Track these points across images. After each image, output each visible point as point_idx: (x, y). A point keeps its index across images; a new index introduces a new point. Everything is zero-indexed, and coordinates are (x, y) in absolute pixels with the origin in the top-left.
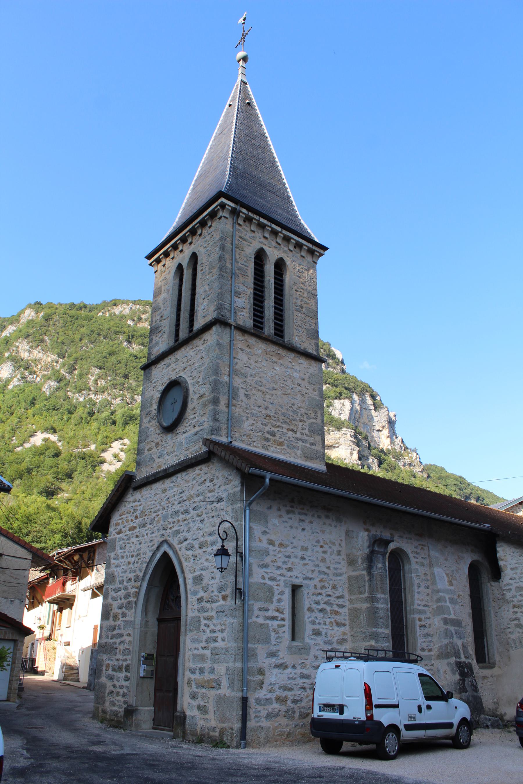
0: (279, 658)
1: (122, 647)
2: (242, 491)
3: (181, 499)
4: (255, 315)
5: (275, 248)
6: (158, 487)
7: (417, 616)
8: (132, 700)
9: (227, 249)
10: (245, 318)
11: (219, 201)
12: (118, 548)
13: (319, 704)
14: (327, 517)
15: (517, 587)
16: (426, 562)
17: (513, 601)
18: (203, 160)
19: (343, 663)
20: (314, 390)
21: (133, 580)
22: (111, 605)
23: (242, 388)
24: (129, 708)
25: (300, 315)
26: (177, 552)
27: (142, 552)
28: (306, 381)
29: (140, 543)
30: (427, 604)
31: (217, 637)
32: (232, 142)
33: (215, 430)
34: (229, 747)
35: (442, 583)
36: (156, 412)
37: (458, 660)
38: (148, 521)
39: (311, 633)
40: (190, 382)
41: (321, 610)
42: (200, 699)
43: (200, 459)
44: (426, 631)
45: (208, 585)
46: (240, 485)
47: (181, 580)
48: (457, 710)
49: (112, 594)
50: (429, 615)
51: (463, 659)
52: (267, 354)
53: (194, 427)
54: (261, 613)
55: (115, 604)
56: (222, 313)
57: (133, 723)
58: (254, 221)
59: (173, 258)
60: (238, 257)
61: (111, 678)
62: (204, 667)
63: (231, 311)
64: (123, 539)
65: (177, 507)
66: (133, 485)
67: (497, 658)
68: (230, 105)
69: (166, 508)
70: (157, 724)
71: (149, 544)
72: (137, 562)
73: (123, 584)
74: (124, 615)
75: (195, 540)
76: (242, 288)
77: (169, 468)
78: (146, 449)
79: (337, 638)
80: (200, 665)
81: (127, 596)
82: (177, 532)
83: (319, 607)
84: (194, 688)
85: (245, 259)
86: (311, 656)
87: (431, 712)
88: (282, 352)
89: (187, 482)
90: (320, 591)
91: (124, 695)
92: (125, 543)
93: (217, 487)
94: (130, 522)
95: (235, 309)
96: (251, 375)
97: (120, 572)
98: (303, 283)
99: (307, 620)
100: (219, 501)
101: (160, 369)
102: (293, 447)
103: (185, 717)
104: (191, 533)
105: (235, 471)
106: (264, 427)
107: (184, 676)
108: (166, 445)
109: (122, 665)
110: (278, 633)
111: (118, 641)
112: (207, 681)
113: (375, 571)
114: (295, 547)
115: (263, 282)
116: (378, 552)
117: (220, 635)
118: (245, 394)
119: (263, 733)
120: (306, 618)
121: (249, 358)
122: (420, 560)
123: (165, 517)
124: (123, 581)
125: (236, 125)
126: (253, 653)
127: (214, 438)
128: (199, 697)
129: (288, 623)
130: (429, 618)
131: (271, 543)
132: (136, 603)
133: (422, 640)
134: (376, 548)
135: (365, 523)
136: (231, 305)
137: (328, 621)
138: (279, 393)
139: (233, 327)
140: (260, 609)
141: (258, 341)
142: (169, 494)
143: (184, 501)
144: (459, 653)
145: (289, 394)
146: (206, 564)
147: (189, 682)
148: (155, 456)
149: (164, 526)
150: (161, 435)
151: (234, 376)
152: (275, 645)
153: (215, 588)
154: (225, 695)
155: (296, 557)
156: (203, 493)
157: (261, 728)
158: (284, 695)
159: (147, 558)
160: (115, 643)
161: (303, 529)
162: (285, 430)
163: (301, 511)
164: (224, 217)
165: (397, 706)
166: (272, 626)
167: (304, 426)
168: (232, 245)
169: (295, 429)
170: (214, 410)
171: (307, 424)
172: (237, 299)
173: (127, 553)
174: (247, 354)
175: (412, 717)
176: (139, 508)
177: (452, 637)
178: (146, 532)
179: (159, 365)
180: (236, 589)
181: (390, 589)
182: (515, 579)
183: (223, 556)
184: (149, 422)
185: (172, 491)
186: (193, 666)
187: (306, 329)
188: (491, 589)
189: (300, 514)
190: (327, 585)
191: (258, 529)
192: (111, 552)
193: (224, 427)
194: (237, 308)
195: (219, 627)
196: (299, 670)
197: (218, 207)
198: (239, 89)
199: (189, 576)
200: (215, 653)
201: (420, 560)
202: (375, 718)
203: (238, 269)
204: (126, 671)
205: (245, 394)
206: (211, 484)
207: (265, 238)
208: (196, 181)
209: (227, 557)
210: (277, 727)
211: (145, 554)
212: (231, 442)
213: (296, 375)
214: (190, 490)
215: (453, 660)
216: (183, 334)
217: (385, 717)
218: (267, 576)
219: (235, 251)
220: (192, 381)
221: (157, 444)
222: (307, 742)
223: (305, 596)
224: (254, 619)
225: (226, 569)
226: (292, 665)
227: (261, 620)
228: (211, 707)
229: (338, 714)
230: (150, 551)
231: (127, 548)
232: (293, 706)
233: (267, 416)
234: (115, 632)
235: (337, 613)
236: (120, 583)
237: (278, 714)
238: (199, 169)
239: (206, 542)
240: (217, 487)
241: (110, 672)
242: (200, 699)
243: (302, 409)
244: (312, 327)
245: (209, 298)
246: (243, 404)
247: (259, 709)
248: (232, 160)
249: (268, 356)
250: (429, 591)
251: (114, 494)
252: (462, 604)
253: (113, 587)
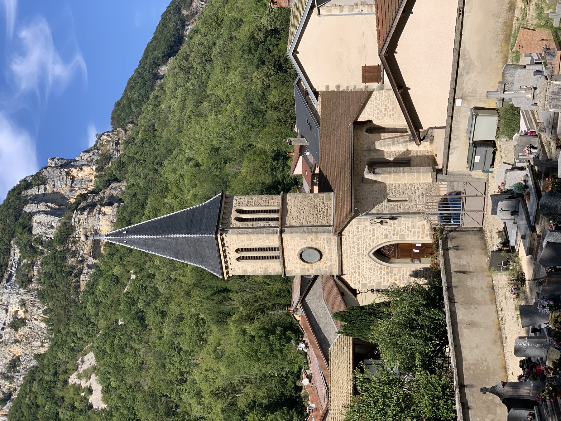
51: (408, 139)
81: (387, 274)
82: (366, 249)
84: (424, 236)
117: (407, 225)
123: (358, 255)
129: (401, 203)
147: (422, 238)
196: (417, 199)
200: (413, 227)
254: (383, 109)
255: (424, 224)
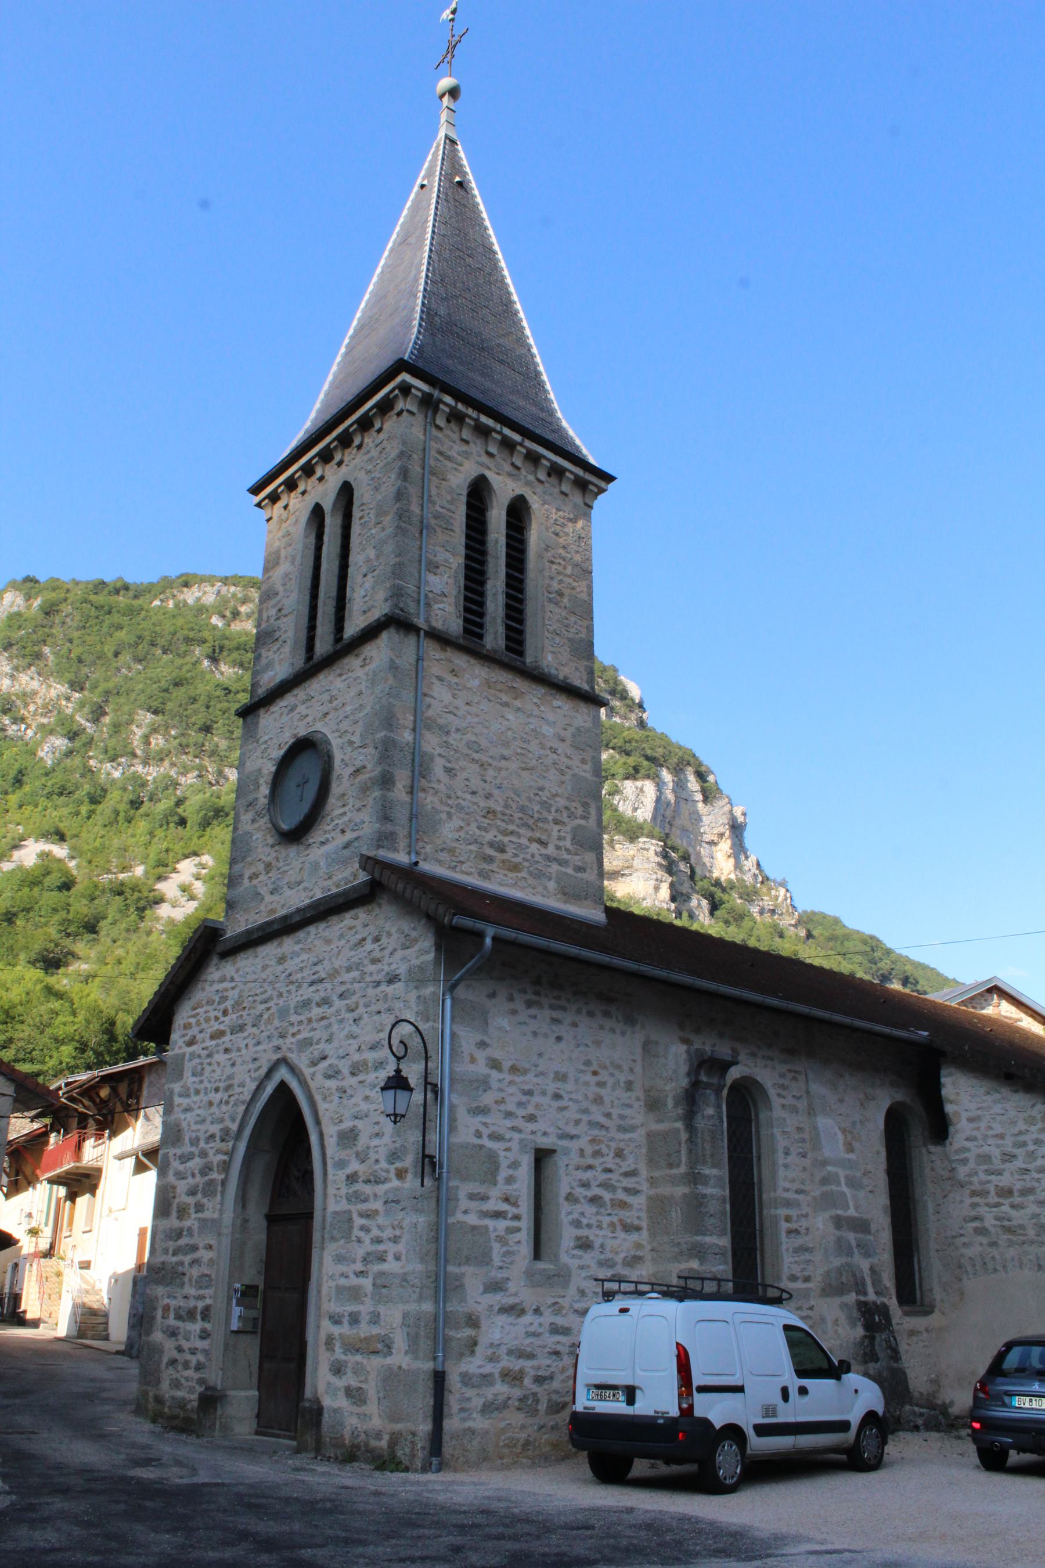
0: (508, 1294)
1: (195, 1272)
2: (437, 961)
3: (315, 977)
4: (466, 609)
5: (510, 475)
6: (269, 951)
7: (782, 1212)
8: (215, 1377)
9: (412, 474)
10: (447, 614)
11: (399, 379)
12: (187, 1074)
13: (587, 1385)
14: (607, 1014)
15: (979, 1156)
16: (802, 1105)
17: (971, 1183)
18: (367, 296)
19: (635, 1305)
20: (583, 761)
21: (218, 1138)
22: (174, 1188)
23: (440, 755)
24: (209, 1393)
25: (557, 610)
26: (306, 1082)
27: (236, 1081)
28: (568, 742)
29: (233, 1065)
30: (803, 1187)
31: (385, 1252)
32: (425, 261)
33: (385, 839)
34: (407, 1470)
35: (834, 1147)
36: (266, 801)
37: (862, 1298)
38: (249, 1021)
39: (572, 1244)
40: (335, 741)
41: (594, 1200)
42: (349, 1374)
43: (355, 896)
44: (799, 1241)
45: (368, 1148)
46: (433, 949)
47: (314, 1139)
48: (858, 1396)
49: (176, 1165)
50: (805, 1209)
51: (871, 1297)
52: (489, 687)
53: (343, 832)
54: (474, 1205)
55: (182, 1186)
56: (401, 605)
57: (218, 1424)
58: (467, 420)
59: (304, 493)
60: (434, 492)
61: (173, 1333)
62: (359, 1312)
63: (419, 601)
64: (199, 1056)
65: (307, 992)
66: (220, 948)
67: (938, 1294)
68: (422, 186)
69: (285, 994)
70: (265, 1424)
71: (251, 1066)
72: (227, 1103)
73: (197, 1145)
74: (199, 1208)
75: (343, 1057)
76: (441, 556)
77: (292, 914)
78: (246, 876)
79: (622, 1256)
80: (351, 1308)
81: (206, 1169)
82: (307, 1043)
83: (589, 1194)
84: (339, 1354)
85: (449, 498)
86: (572, 1290)
87: (806, 1399)
88: (520, 684)
89: (328, 942)
90: (590, 1161)
91: (199, 1367)
92: (202, 1064)
93: (387, 952)
94: (212, 1022)
95: (426, 596)
96: (458, 730)
97: (192, 1123)
98: (564, 547)
99: (565, 1219)
100: (390, 982)
101: (277, 715)
102: (539, 875)
103: (319, 1411)
104: (335, 1044)
105: (423, 921)
106: (483, 833)
107: (320, 1329)
108: (285, 868)
109: (196, 1308)
110: (506, 1244)
111: (187, 1259)
112: (365, 1338)
113: (700, 1123)
114: (542, 1074)
115: (483, 543)
116: (708, 1086)
117: (391, 1248)
118: (445, 767)
119: (475, 1443)
120: (564, 1213)
121: (454, 696)
122: (789, 1101)
123: (283, 1013)
124: (198, 1139)
125: (434, 226)
126: (457, 1283)
127: (384, 854)
128: (349, 1370)
129: (526, 1224)
130: (806, 1216)
131: (495, 1064)
132: (223, 1183)
133: (791, 1259)
134: (704, 1078)
135: (681, 1027)
136: (419, 588)
137: (606, 1220)
138: (514, 765)
139: (422, 632)
140: (472, 1197)
141: (473, 661)
142: (291, 965)
143: (321, 981)
144: (864, 1284)
145: (533, 769)
146: (364, 1107)
147: (330, 1342)
148: (263, 891)
149: (280, 1030)
150: (277, 848)
151: (424, 732)
152: (501, 1268)
153: (382, 1154)
154: (400, 1368)
155: (544, 1093)
156: (359, 964)
157: (472, 1432)
158: (517, 1368)
159: (246, 1093)
160: (182, 1264)
161: (559, 1039)
162: (524, 841)
163: (554, 1001)
164: (408, 411)
165: (740, 1389)
166: (495, 1230)
167: (562, 834)
168: (423, 468)
169: (544, 838)
170: (384, 798)
171: (568, 828)
172: (431, 578)
173: (206, 1084)
174: (449, 686)
175: (770, 1410)
176: (230, 994)
177: (850, 1254)
178: (245, 1042)
179: (273, 709)
180: (424, 1156)
181: (730, 1158)
182: (975, 1139)
183: (399, 1092)
184: (253, 821)
185: (297, 960)
186: (338, 1310)
187: (569, 640)
188: (929, 1160)
189: (552, 1007)
190: (605, 1150)
191: (468, 1038)
192: (175, 1082)
193: (402, 832)
194: (431, 595)
195: (389, 1233)
196: (548, 1318)
197: (397, 392)
198: (441, 152)
199: (331, 1131)
200: (382, 1284)
201: (789, 1101)
202: (698, 1412)
203: (436, 518)
204: (203, 1319)
205: (445, 767)
206: (375, 946)
207: (490, 455)
208: (352, 337)
209: (406, 1094)
210: (503, 1430)
211: (242, 1085)
212: (416, 863)
213: (547, 730)
214: (334, 960)
215: (852, 1298)
216: (323, 646)
217: (716, 1410)
218: (486, 1132)
219: (429, 480)
220: (339, 741)
221: (268, 867)
222: (563, 1460)
223: (562, 1171)
224: (459, 1217)
225: (403, 1116)
226: (534, 1307)
227: (472, 1219)
228: (372, 1390)
229: (624, 1404)
230: (253, 1080)
231: (207, 1073)
232: (535, 1388)
233: (488, 812)
234: (182, 1242)
235: (623, 1205)
236: (192, 1144)
237: (505, 1405)
238: (358, 315)
239: (365, 1063)
240: (387, 952)
241: (172, 1321)
242: (349, 1374)
243: (557, 799)
244: (580, 635)
245: (375, 573)
246: (441, 787)
247: (467, 1395)
248: (424, 297)
249: (491, 691)
250: (807, 1163)
251: (181, 966)
252: (870, 1188)
253: (178, 1151)
254: (1005, 1181)
255: (388, 1347)
